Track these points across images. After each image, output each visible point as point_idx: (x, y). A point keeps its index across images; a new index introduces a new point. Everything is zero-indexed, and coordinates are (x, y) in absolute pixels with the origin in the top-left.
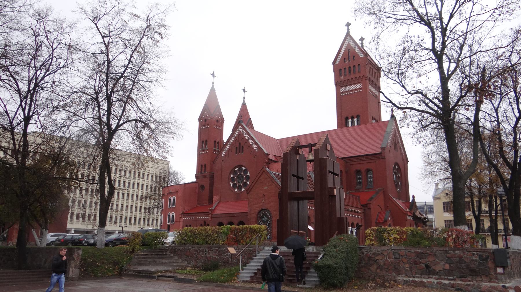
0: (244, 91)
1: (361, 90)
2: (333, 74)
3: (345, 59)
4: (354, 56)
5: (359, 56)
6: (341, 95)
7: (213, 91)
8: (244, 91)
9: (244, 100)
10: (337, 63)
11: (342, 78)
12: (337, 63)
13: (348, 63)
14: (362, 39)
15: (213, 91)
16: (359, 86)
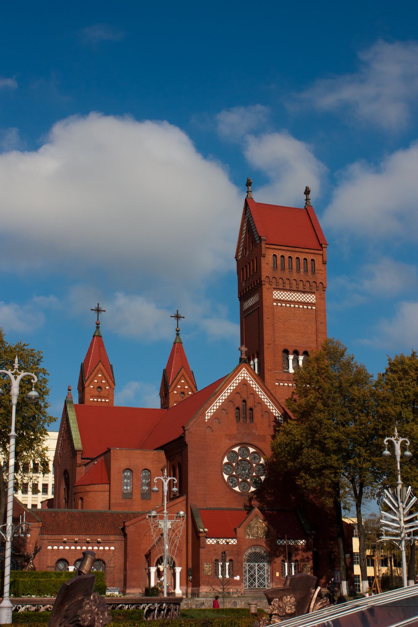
2: (237, 276)
7: (97, 337)
8: (178, 317)
15: (97, 337)
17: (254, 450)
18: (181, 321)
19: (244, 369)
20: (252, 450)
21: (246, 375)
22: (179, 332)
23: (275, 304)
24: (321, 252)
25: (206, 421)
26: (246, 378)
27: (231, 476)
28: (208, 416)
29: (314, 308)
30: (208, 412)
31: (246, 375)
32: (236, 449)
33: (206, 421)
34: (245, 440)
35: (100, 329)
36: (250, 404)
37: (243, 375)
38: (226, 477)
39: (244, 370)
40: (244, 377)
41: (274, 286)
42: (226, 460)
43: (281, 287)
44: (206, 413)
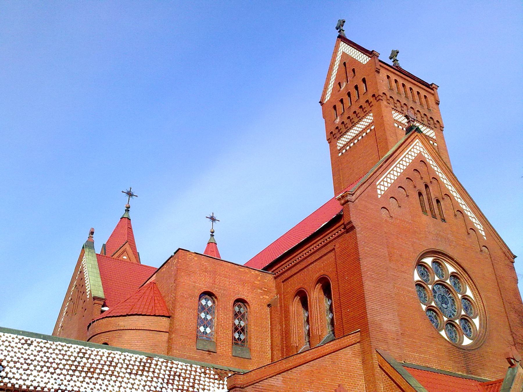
0: (213, 219)
1: (372, 128)
3: (339, 84)
4: (354, 70)
5: (362, 63)
6: (340, 154)
7: (126, 220)
8: (213, 219)
9: (212, 235)
10: (328, 97)
11: (338, 120)
12: (328, 97)
13: (346, 86)
14: (394, 55)
15: (126, 220)
16: (369, 119)
17: (455, 271)
18: (216, 224)
19: (417, 140)
20: (451, 269)
21: (422, 150)
22: (213, 234)
23: (396, 125)
24: (432, 92)
25: (379, 196)
26: (423, 154)
27: (430, 309)
28: (381, 190)
29: (435, 144)
30: (379, 184)
31: (422, 150)
32: (429, 261)
33: (379, 196)
34: (440, 248)
35: (130, 213)
36: (434, 192)
37: (418, 148)
38: (424, 307)
39: (418, 142)
40: (421, 152)
41: (393, 107)
42: (417, 277)
43: (399, 109)
44: (377, 183)
